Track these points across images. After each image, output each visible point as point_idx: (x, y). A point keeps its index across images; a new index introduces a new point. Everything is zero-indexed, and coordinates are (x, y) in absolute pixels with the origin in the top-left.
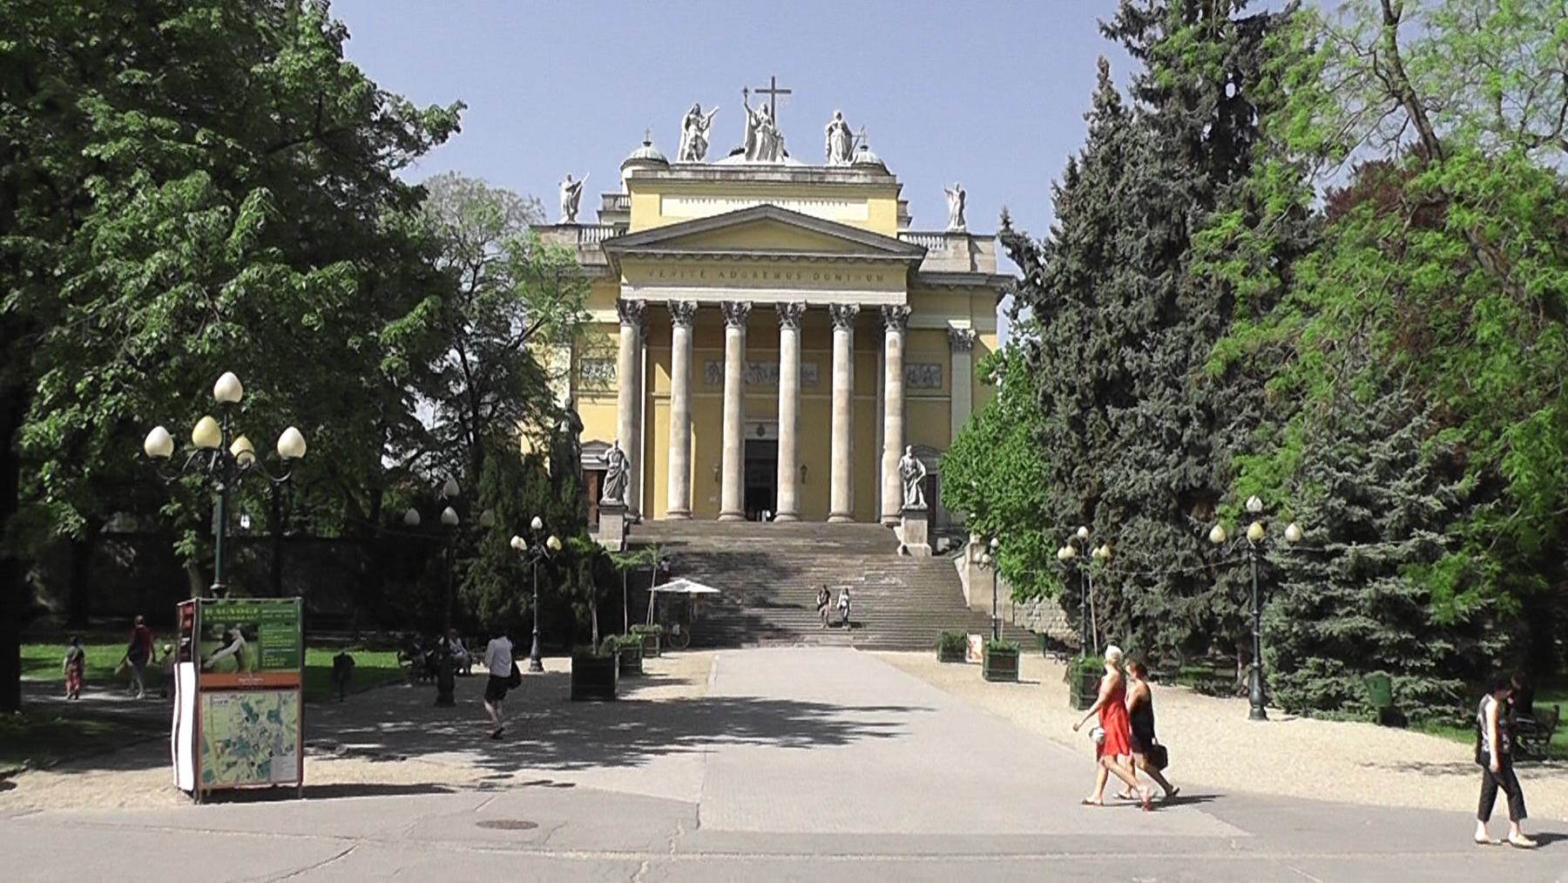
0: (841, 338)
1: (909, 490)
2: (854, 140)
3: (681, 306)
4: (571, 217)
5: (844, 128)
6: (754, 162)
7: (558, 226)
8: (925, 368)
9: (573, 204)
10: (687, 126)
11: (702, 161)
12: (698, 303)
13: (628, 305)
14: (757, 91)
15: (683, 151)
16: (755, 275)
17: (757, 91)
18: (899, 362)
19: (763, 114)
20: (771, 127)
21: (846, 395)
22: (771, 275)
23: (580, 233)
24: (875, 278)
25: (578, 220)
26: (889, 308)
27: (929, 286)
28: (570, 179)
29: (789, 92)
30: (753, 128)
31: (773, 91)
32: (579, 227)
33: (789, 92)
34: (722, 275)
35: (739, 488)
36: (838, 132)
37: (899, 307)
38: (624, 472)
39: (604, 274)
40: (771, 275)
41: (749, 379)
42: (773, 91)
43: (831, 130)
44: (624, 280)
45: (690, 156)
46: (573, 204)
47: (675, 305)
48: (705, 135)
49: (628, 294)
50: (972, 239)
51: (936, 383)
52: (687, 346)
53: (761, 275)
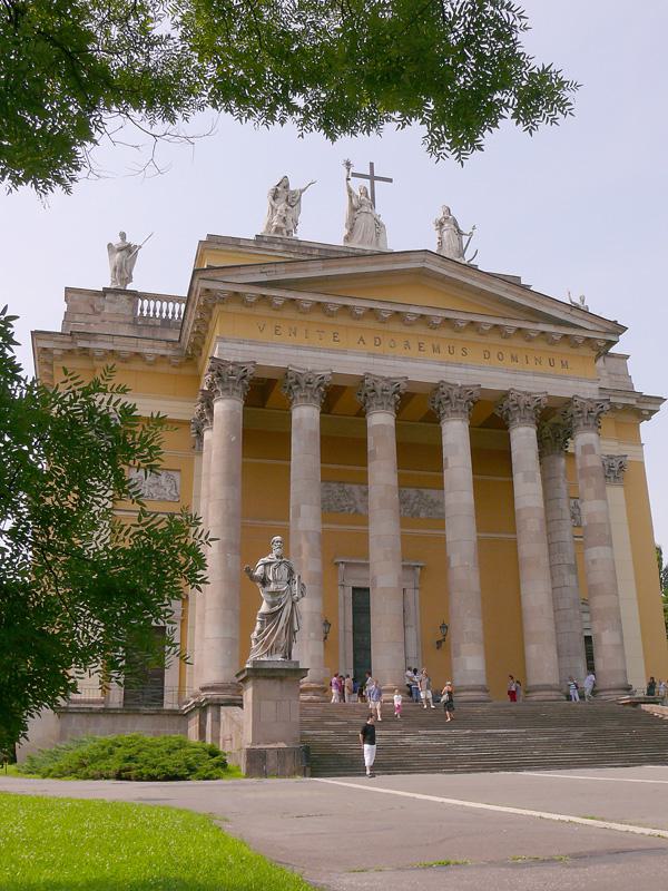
2: (465, 239)
7: (106, 291)
9: (123, 271)
16: (407, 346)
19: (363, 197)
22: (428, 346)
24: (558, 362)
29: (391, 180)
32: (135, 295)
33: (391, 180)
34: (361, 339)
39: (169, 353)
40: (428, 346)
43: (441, 224)
46: (123, 271)
53: (415, 347)
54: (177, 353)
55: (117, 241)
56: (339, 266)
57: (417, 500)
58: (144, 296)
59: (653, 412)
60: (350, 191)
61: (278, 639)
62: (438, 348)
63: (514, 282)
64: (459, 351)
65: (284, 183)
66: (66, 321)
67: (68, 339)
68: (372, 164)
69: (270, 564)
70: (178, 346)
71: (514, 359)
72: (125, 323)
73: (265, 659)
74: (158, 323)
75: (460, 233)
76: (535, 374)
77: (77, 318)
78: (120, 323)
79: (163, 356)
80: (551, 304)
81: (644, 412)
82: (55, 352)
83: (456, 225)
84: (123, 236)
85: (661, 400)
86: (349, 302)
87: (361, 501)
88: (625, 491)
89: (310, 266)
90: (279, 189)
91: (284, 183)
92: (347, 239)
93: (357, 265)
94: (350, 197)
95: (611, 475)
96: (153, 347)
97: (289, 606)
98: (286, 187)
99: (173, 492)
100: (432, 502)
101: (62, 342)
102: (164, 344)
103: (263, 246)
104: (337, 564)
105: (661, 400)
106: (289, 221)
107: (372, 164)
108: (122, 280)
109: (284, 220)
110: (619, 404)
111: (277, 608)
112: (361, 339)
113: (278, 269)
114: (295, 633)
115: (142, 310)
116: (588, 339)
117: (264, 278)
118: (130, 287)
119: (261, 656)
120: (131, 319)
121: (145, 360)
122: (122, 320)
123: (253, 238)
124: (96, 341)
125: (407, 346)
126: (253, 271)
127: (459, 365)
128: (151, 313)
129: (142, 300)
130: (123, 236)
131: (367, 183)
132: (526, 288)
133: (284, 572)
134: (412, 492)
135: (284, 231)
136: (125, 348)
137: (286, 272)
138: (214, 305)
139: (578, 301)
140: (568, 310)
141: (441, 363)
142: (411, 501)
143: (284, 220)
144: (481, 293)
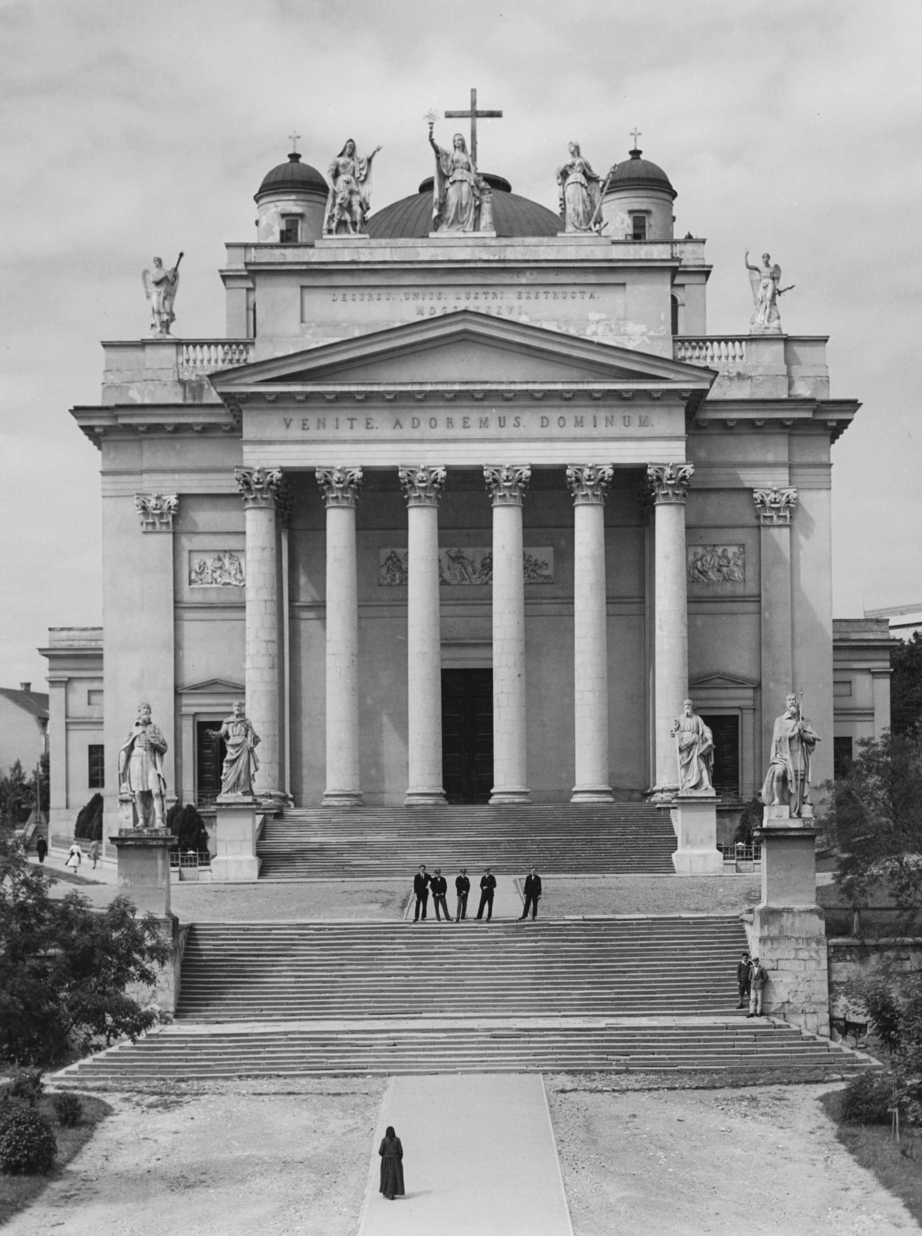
4: (166, 325)
8: (720, 551)
14: (449, 115)
17: (449, 115)
25: (177, 331)
27: (723, 423)
28: (159, 262)
31: (475, 114)
32: (179, 344)
36: (576, 176)
41: (447, 575)
50: (788, 340)
51: (737, 575)
58: (188, 343)
59: (844, 424)
81: (830, 424)
85: (854, 405)
87: (449, 568)
94: (438, 159)
99: (238, 576)
100: (536, 565)
131: (463, 127)
133: (240, 728)
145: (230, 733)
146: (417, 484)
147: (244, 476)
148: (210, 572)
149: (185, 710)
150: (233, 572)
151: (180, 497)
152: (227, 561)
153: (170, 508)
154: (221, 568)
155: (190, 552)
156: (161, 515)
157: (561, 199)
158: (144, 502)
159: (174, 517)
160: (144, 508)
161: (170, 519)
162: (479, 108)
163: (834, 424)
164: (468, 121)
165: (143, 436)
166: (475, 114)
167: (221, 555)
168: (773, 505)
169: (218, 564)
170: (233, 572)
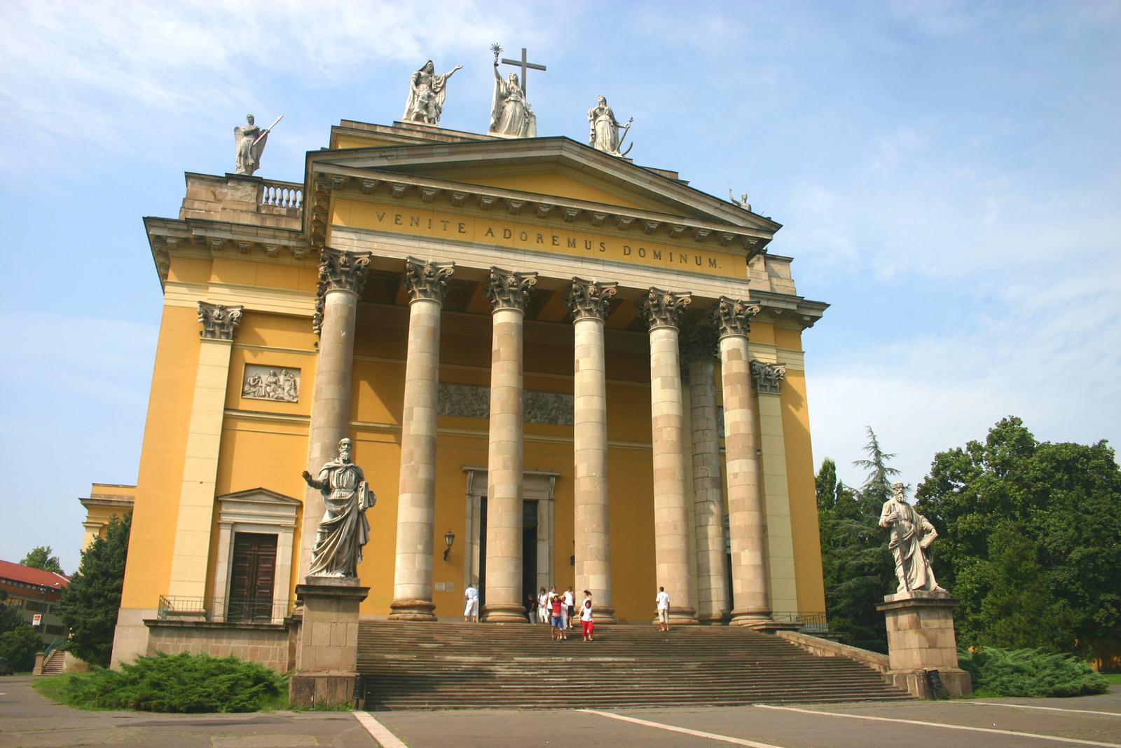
0: (662, 342)
1: (908, 564)
2: (621, 132)
3: (427, 269)
5: (611, 115)
6: (502, 135)
7: (230, 177)
9: (253, 154)
10: (417, 83)
11: (439, 125)
12: (455, 267)
13: (343, 259)
15: (410, 111)
18: (746, 380)
19: (513, 84)
20: (523, 101)
21: (675, 423)
23: (260, 192)
26: (730, 303)
29: (543, 68)
30: (502, 97)
32: (260, 183)
33: (543, 68)
35: (517, 567)
37: (742, 303)
38: (361, 514)
39: (292, 244)
42: (524, 65)
43: (596, 116)
44: (336, 220)
45: (419, 117)
47: (417, 267)
48: (439, 99)
49: (341, 241)
52: (434, 330)
54: (300, 244)
55: (245, 126)
56: (467, 153)
57: (556, 405)
59: (816, 318)
60: (498, 77)
61: (339, 552)
62: (574, 243)
63: (672, 180)
64: (596, 246)
65: (429, 69)
66: (184, 208)
67: (184, 227)
68: (524, 51)
69: (335, 468)
70: (301, 236)
71: (657, 256)
72: (247, 212)
73: (324, 574)
74: (284, 212)
75: (615, 125)
76: (679, 273)
77: (196, 205)
78: (242, 211)
79: (286, 247)
80: (698, 198)
82: (169, 241)
83: (611, 115)
84: (251, 120)
85: (823, 306)
86: (476, 191)
88: (781, 400)
89: (435, 151)
90: (423, 74)
91: (429, 69)
92: (494, 128)
93: (487, 151)
94: (499, 84)
95: (767, 384)
96: (275, 237)
97: (354, 516)
98: (431, 72)
99: (292, 392)
101: (177, 230)
102: (287, 235)
103: (402, 133)
104: (466, 472)
105: (823, 306)
106: (432, 108)
107: (524, 51)
108: (246, 166)
109: (426, 107)
110: (779, 309)
111: (339, 518)
112: (490, 231)
113: (400, 153)
114: (361, 546)
115: (267, 199)
116: (739, 236)
117: (384, 163)
118: (256, 174)
119: (321, 571)
120: (254, 208)
121: (265, 251)
122: (244, 208)
123: (391, 124)
124: (213, 230)
125: (540, 239)
126: (372, 155)
127: (596, 261)
128: (277, 202)
129: (268, 188)
130: (251, 120)
131: (518, 70)
132: (683, 184)
133: (349, 477)
134: (452, 388)
135: (425, 118)
136: (245, 238)
137: (409, 156)
138: (330, 192)
139: (739, 199)
140: (718, 206)
141: (576, 259)
142: (550, 408)
143: (426, 107)
144: (622, 184)
145: (334, 483)
146: (506, 288)
147: (331, 258)
148: (264, 385)
149: (225, 519)
150: (287, 388)
151: (246, 313)
152: (282, 378)
153: (232, 320)
154: (275, 383)
155: (247, 365)
156: (222, 326)
157: (593, 130)
158: (206, 311)
159: (235, 329)
160: (206, 319)
161: (231, 330)
162: (528, 61)
163: (808, 319)
164: (520, 68)
165: (214, 253)
166: (524, 65)
167: (277, 371)
168: (768, 377)
169: (273, 379)
170: (287, 388)
